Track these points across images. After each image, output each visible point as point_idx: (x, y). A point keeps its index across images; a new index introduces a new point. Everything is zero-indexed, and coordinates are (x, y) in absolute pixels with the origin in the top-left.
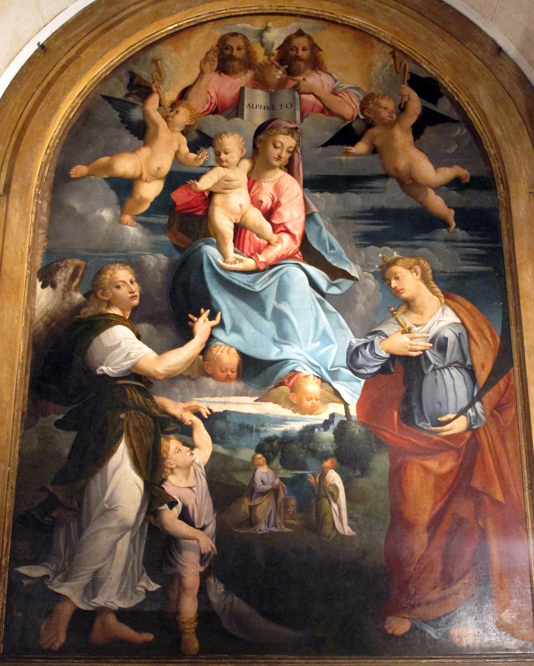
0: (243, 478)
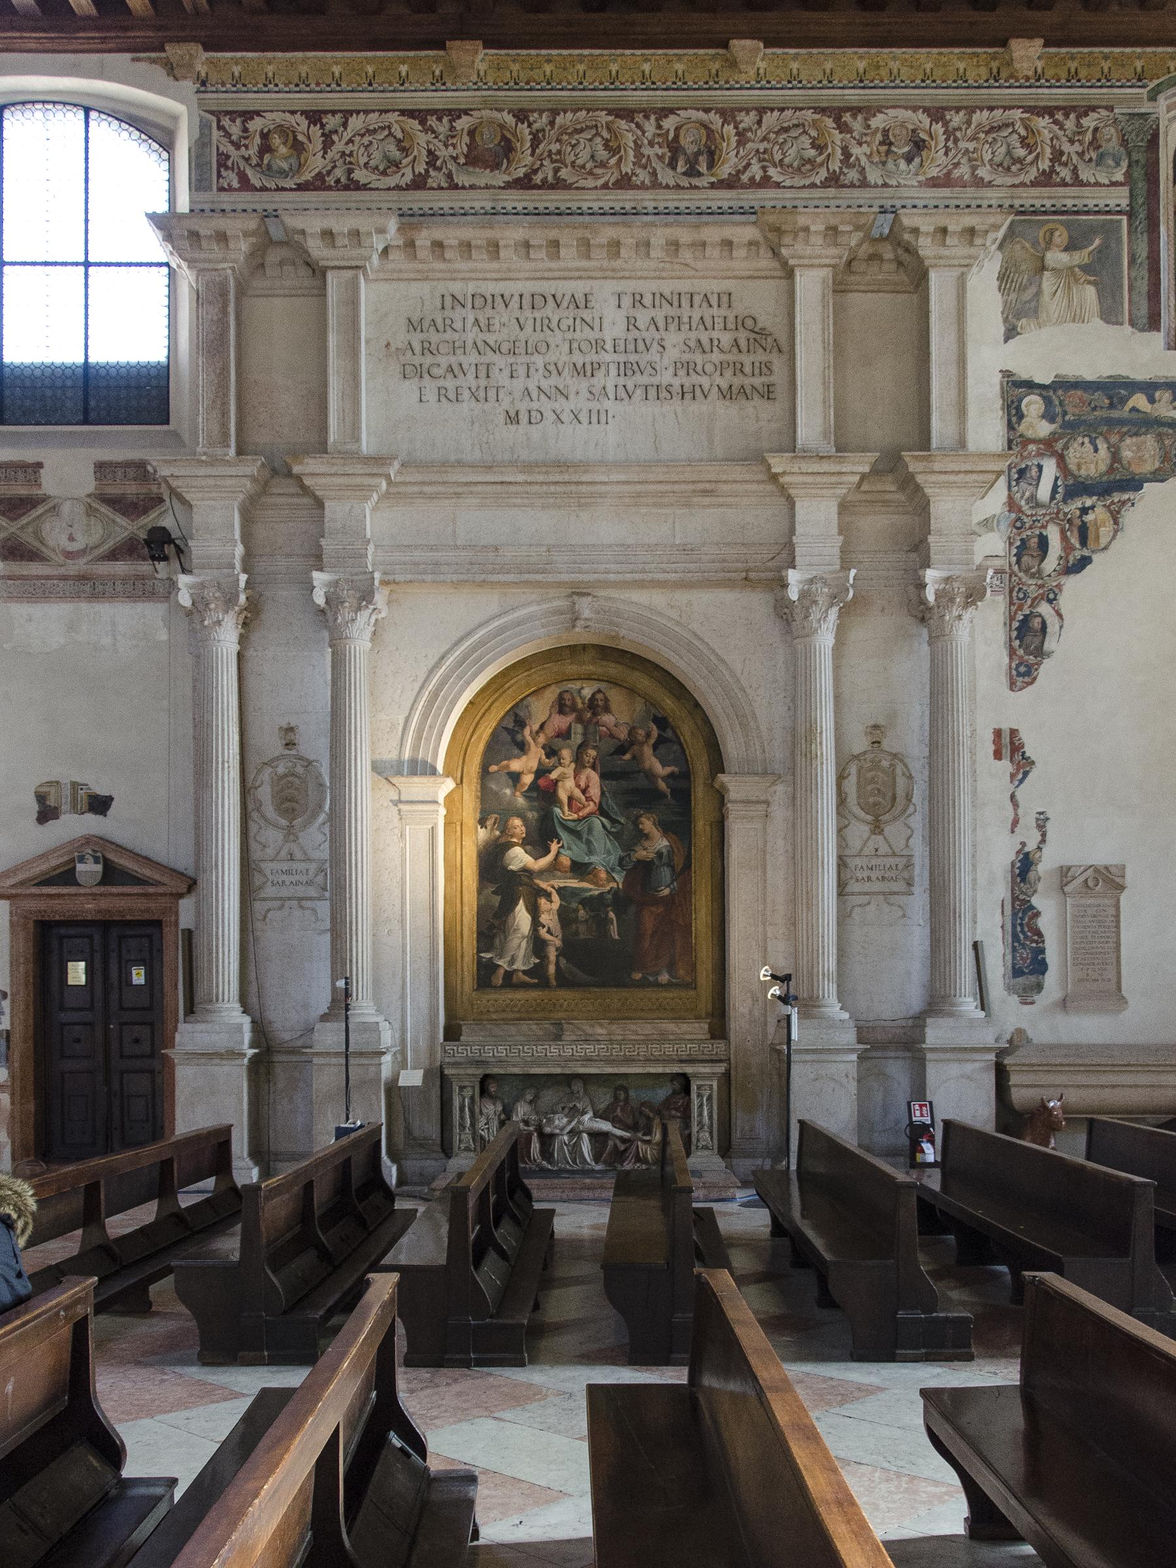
0: (573, 915)
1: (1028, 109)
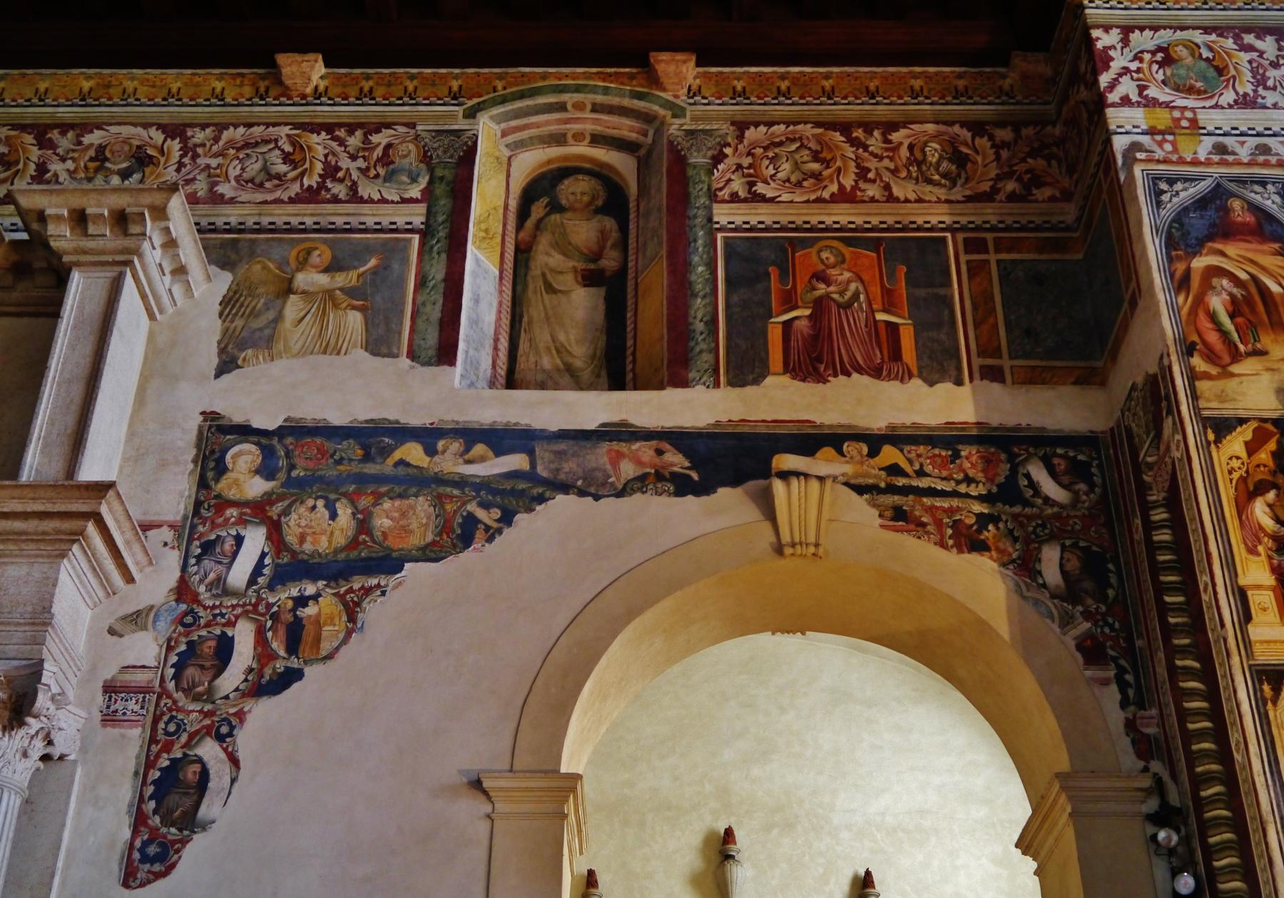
1: (296, 126)
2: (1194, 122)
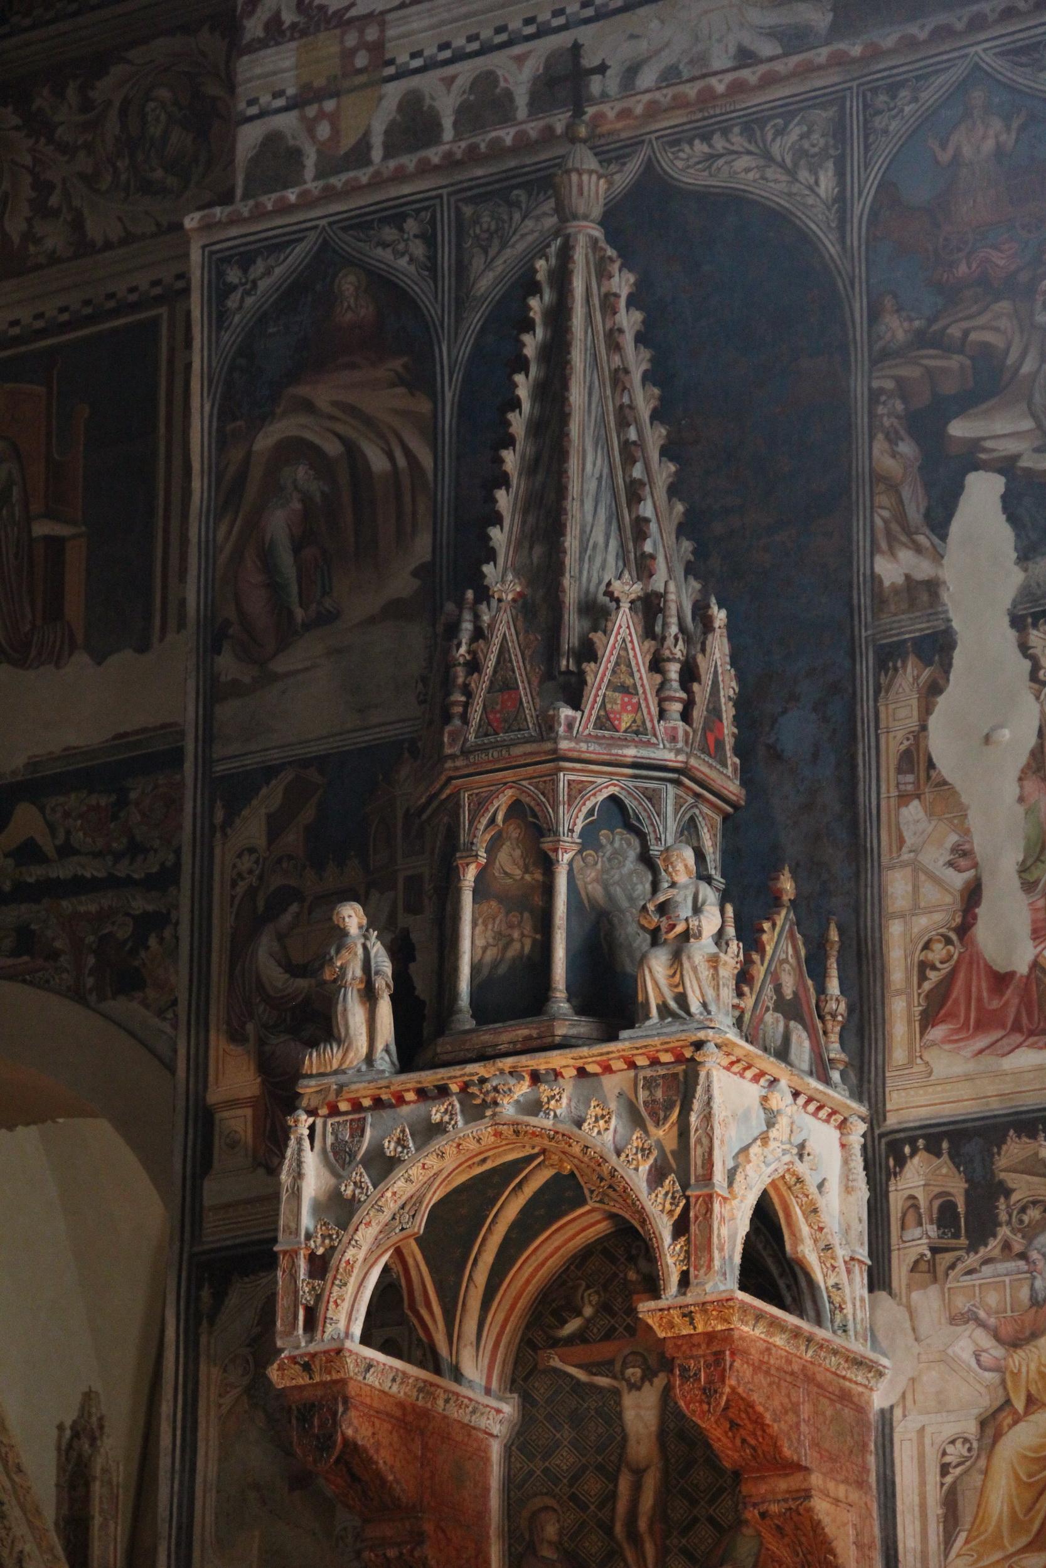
2: (377, 48)
